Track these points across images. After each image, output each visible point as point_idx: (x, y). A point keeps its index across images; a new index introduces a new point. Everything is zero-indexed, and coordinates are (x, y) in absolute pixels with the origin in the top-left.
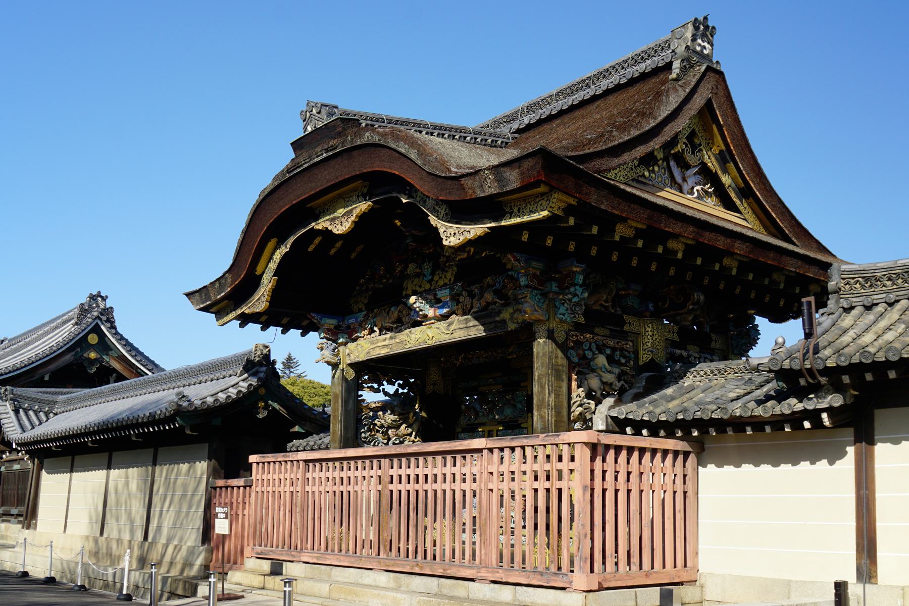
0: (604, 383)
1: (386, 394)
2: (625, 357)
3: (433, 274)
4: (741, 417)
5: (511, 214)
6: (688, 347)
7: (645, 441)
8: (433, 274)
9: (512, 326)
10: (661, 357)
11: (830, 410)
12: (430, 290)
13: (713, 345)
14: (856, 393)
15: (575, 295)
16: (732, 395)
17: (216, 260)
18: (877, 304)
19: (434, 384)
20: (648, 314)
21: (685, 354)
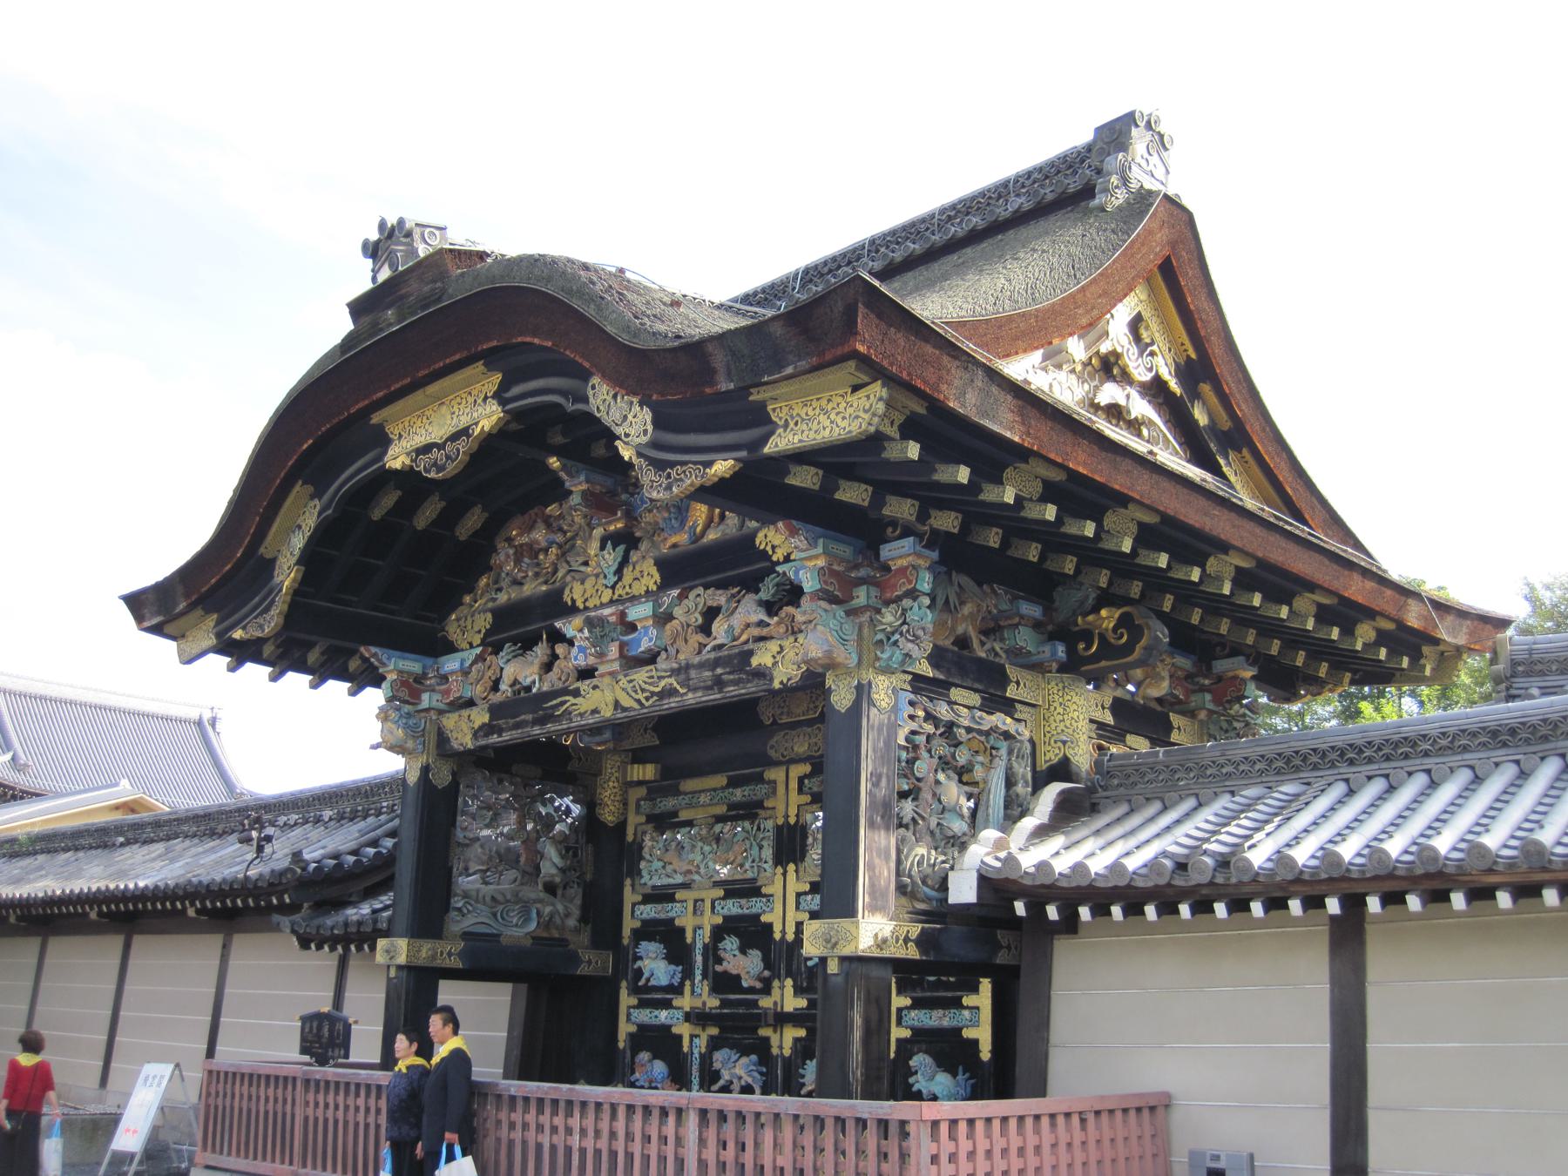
3: (619, 572)
8: (619, 572)
20: (1055, 666)
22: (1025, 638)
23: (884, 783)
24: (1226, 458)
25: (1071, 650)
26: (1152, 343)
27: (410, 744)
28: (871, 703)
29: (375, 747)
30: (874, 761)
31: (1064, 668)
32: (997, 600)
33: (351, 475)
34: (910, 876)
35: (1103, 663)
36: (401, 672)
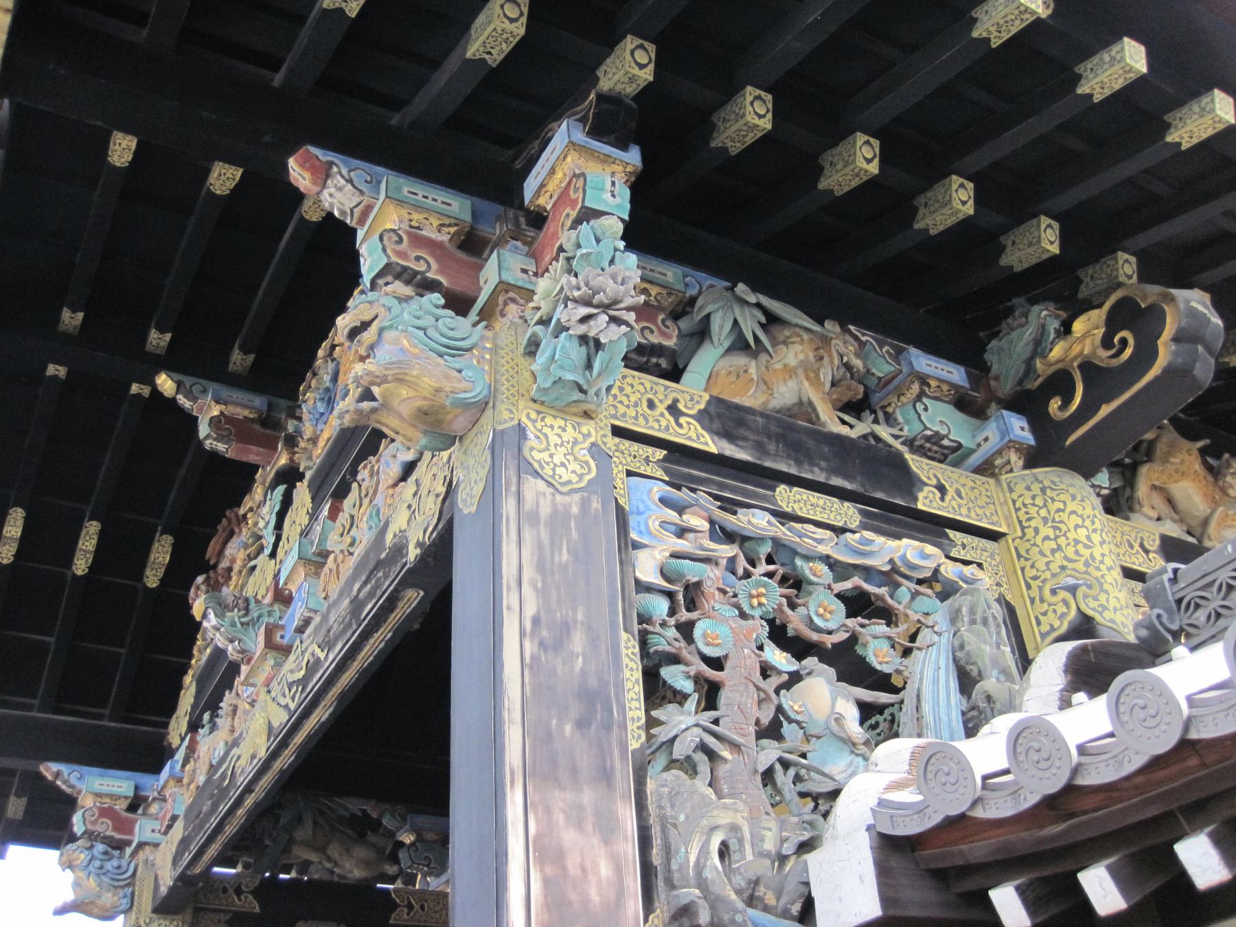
22: (941, 418)
23: (578, 642)
27: (108, 898)
28: (526, 468)
29: (62, 911)
30: (542, 593)
31: (1034, 459)
34: (702, 884)
35: (1105, 410)
36: (98, 795)
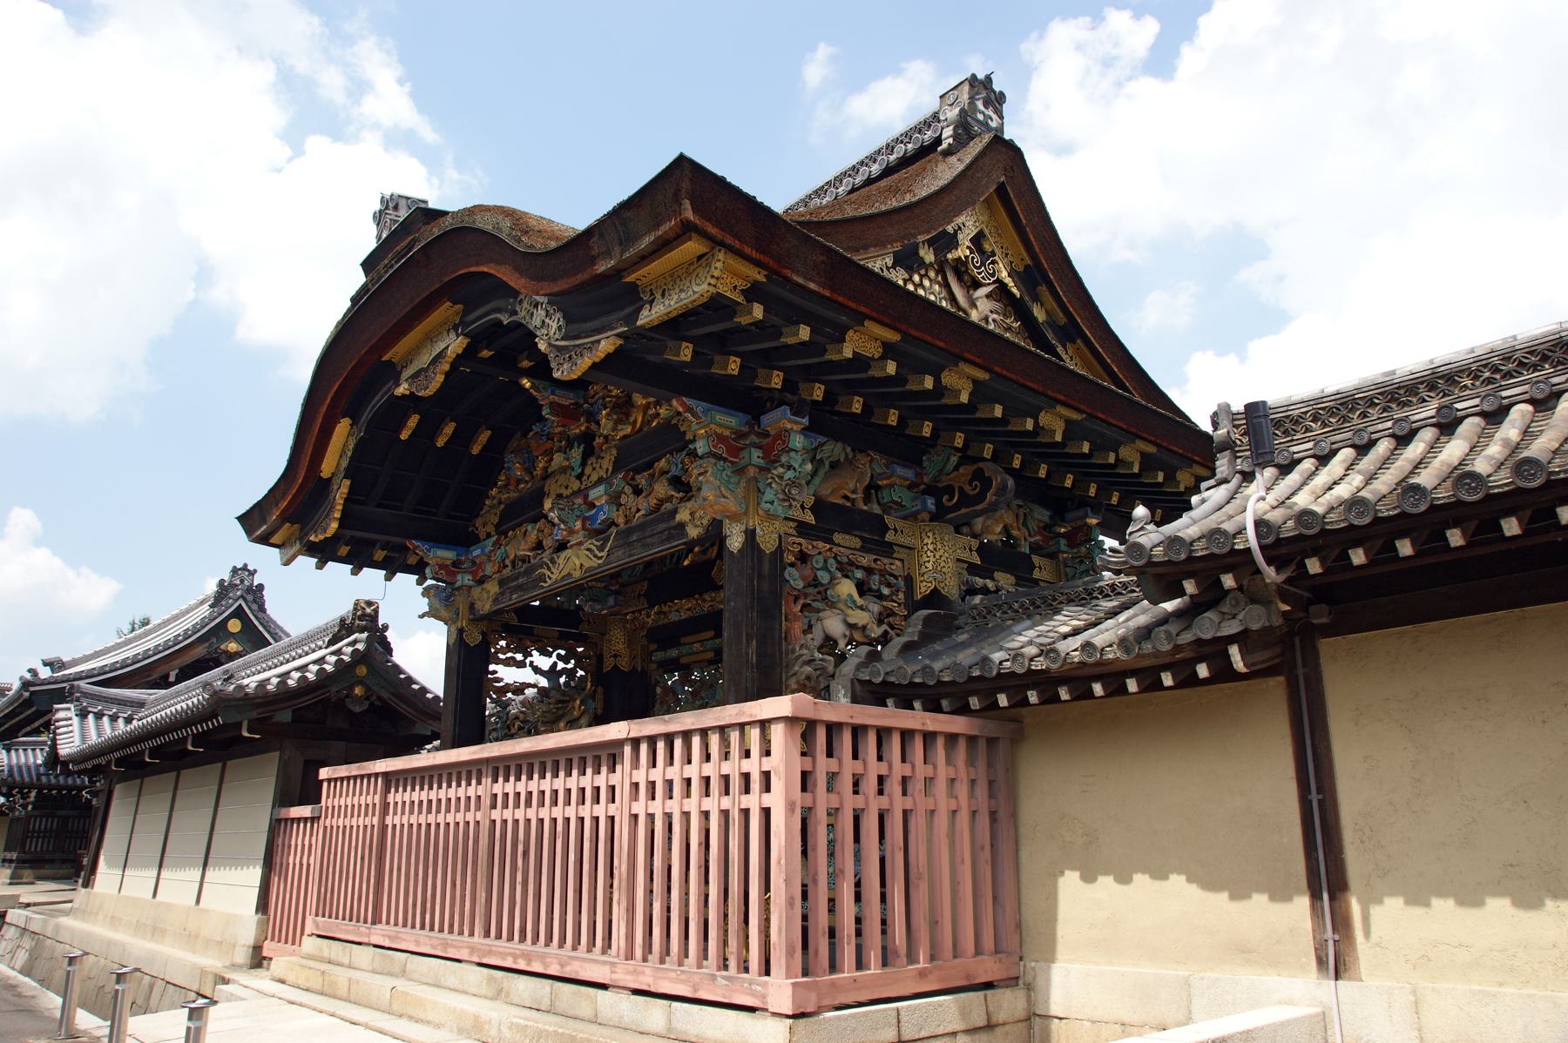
0: (852, 626)
1: (537, 670)
2: (889, 585)
3: (584, 464)
4: (1082, 664)
5: (651, 303)
6: (996, 575)
7: (917, 719)
8: (584, 464)
9: (693, 532)
10: (951, 589)
11: (1240, 638)
12: (579, 490)
13: (1036, 574)
14: (1287, 608)
15: (790, 467)
16: (1065, 629)
17: (264, 462)
18: (1299, 461)
19: (615, 656)
20: (925, 516)
21: (990, 584)
22: (899, 495)
24: (1064, 347)
25: (938, 503)
26: (993, 254)
27: (444, 613)
29: (421, 617)
31: (935, 517)
32: (870, 465)
33: (378, 400)
35: (964, 511)
